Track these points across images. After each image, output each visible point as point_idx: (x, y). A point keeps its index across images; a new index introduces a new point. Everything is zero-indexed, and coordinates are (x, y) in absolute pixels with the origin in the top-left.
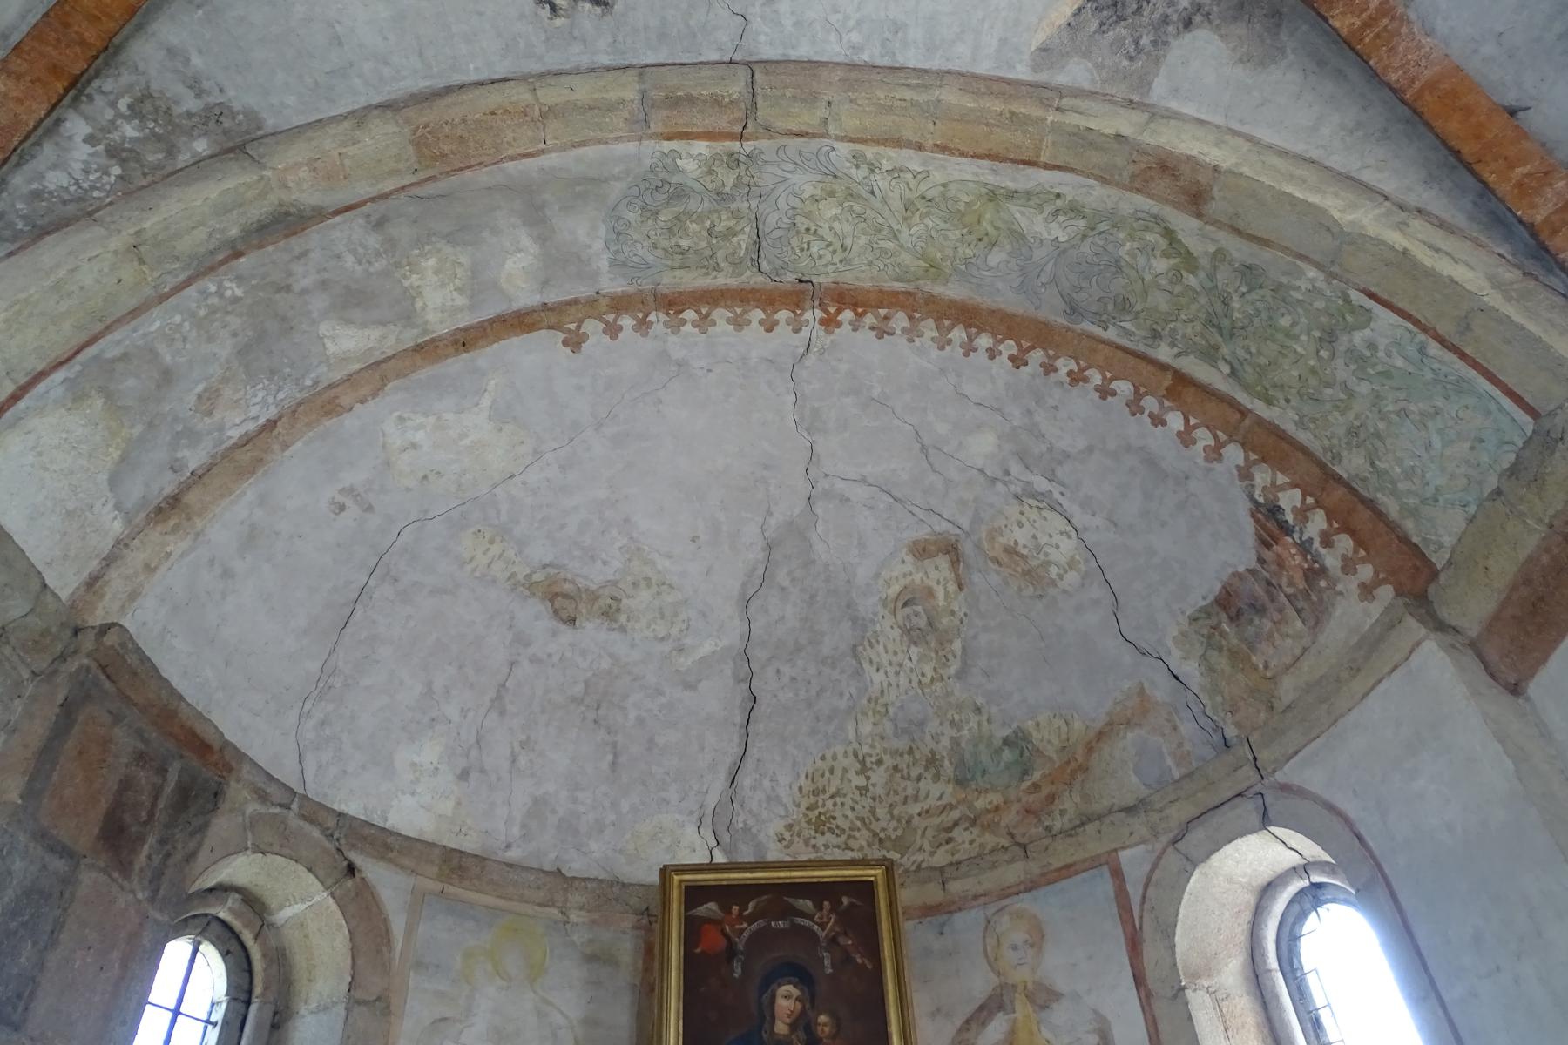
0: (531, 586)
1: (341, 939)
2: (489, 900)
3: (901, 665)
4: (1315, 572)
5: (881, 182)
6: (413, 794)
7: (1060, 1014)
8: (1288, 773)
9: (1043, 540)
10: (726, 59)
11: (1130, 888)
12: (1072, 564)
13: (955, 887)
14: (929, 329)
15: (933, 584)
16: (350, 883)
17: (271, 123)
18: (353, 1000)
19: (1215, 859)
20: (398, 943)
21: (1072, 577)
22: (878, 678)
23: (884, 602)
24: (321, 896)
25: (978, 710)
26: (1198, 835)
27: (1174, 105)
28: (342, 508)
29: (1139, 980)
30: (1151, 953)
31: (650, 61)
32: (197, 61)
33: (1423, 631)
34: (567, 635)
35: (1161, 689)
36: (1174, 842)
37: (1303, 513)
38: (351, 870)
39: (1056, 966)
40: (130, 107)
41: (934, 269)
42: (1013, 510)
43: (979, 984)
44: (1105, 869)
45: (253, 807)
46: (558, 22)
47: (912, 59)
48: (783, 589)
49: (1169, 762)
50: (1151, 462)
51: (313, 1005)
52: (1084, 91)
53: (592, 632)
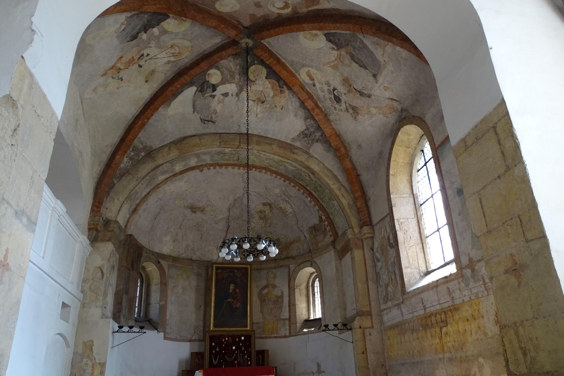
0: (188, 207)
2: (180, 265)
3: (258, 223)
4: (325, 230)
5: (262, 155)
6: (166, 246)
7: (276, 290)
8: (315, 260)
9: (286, 208)
10: (236, 132)
11: (291, 271)
12: (291, 213)
13: (262, 266)
14: (269, 173)
15: (266, 210)
16: (159, 265)
17: (154, 147)
19: (304, 269)
21: (291, 215)
22: (254, 225)
23: (256, 212)
24: (155, 267)
25: (271, 233)
26: (302, 265)
27: (313, 154)
28: (158, 201)
29: (289, 286)
30: (292, 283)
31: (222, 132)
32: (142, 139)
33: (332, 248)
34: (194, 214)
35: (303, 238)
36: (299, 265)
37: (325, 220)
38: (159, 262)
39: (277, 282)
40: (132, 149)
41: (271, 166)
42: (282, 202)
43: (264, 283)
44: (288, 267)
46: (205, 125)
47: (270, 136)
48: (237, 208)
49: (302, 250)
50: (305, 202)
51: (154, 284)
52: (299, 147)
53: (199, 214)
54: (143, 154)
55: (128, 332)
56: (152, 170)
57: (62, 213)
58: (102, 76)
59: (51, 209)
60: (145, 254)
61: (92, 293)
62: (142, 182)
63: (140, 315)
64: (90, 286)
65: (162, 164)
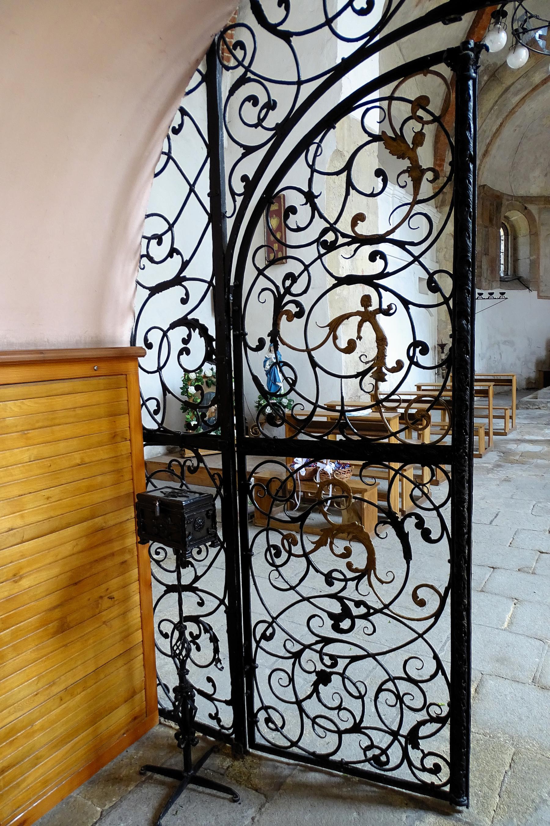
1: (526, 223)
16: (526, 211)
18: (531, 234)
20: (537, 221)
24: (521, 215)
28: (516, 130)
38: (526, 208)
45: (507, 203)
51: (522, 235)
54: (486, 78)
55: (488, 298)
56: (502, 95)
57: (402, 195)
58: (417, 6)
59: (391, 196)
60: (505, 202)
61: (448, 262)
62: (490, 116)
63: (508, 273)
64: (445, 255)
65: (513, 84)
